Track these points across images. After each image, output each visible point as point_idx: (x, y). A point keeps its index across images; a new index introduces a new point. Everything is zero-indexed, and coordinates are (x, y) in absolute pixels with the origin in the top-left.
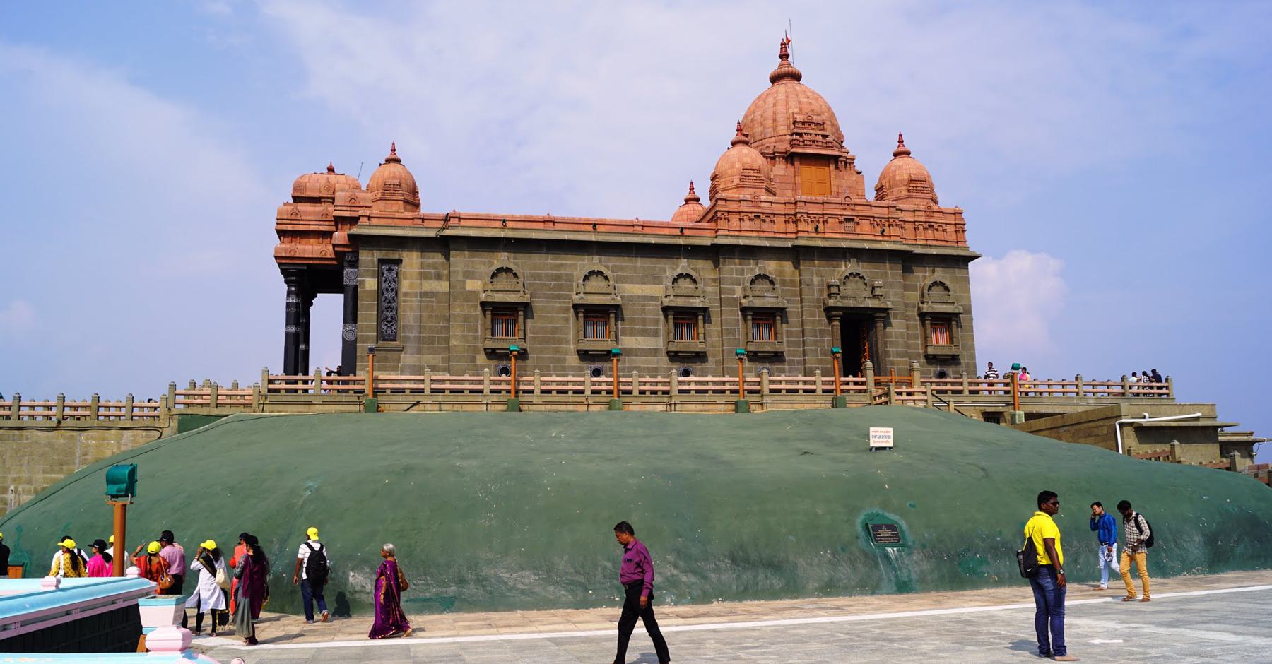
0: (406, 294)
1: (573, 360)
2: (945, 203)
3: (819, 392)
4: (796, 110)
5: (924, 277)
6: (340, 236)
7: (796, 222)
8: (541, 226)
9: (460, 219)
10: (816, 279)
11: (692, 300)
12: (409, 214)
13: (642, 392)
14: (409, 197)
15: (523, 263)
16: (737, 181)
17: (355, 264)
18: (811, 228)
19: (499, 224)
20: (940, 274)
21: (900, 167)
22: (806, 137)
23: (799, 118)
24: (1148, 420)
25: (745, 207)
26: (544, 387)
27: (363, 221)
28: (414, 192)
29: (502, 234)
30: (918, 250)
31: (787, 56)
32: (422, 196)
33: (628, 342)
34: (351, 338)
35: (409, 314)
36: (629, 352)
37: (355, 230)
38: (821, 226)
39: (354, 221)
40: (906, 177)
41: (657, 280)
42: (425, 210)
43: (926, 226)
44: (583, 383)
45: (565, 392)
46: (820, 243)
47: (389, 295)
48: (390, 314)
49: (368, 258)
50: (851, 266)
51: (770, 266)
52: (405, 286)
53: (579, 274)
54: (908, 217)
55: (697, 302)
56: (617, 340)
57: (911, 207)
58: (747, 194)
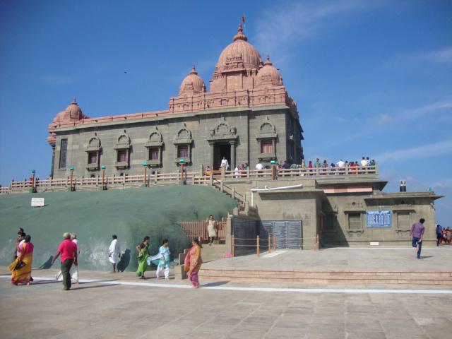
1: (115, 170)
5: (260, 120)
10: (206, 128)
13: (115, 183)
15: (102, 135)
23: (230, 57)
24: (265, 190)
25: (180, 101)
30: (253, 110)
36: (135, 166)
38: (211, 105)
50: (221, 120)
51: (189, 124)
52: (68, 148)
54: (255, 94)
56: (129, 162)
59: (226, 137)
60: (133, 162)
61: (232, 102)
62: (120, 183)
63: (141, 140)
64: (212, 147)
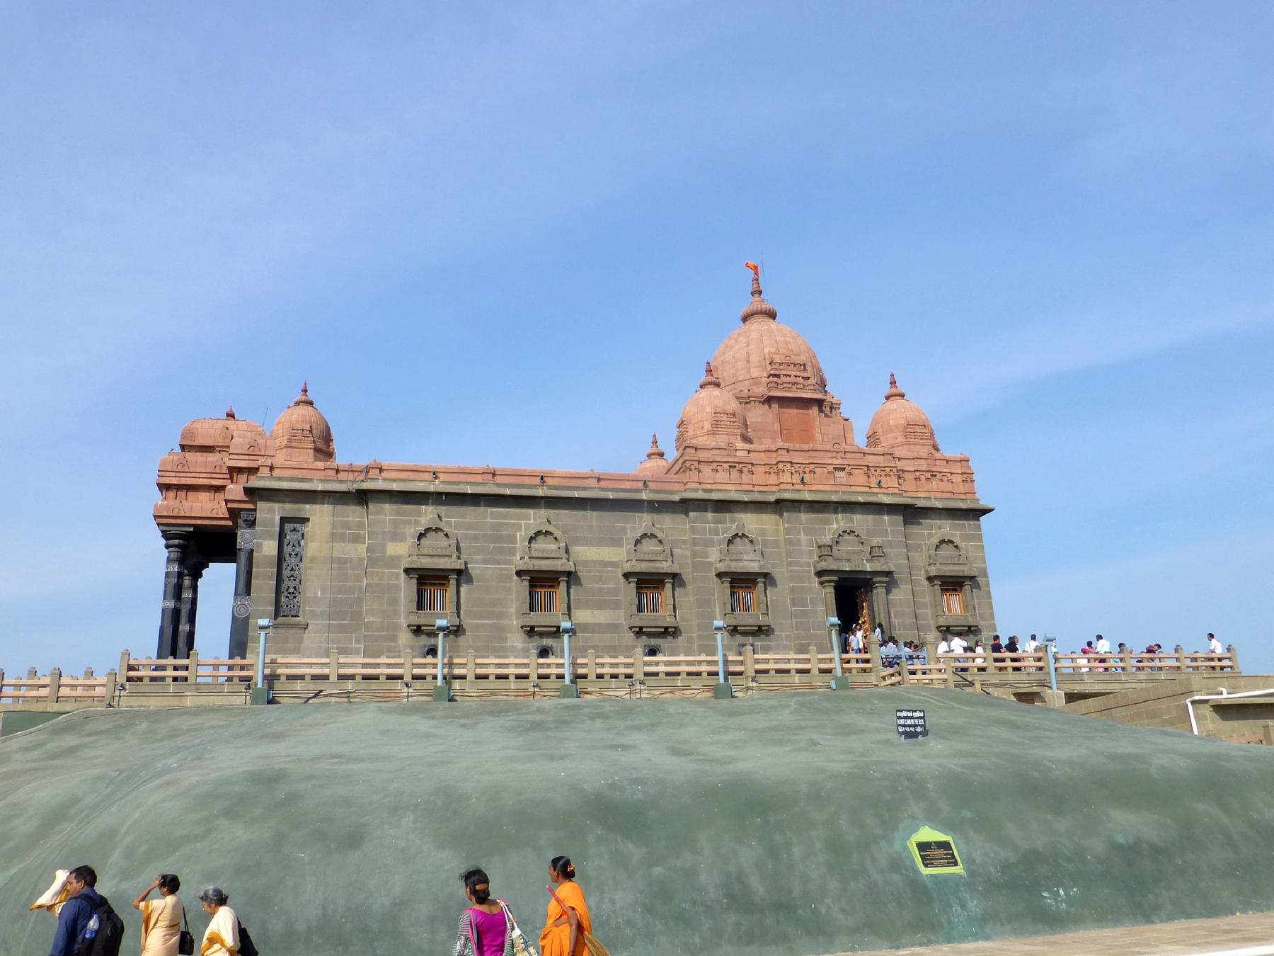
0: (313, 560)
1: (517, 640)
2: (948, 451)
3: (815, 672)
4: (773, 350)
6: (235, 490)
7: (777, 473)
8: (479, 478)
9: (381, 470)
11: (658, 565)
12: (320, 464)
13: (600, 677)
14: (320, 445)
15: (457, 519)
16: (708, 426)
17: (252, 524)
18: (797, 479)
19: (430, 476)
20: (946, 528)
21: (894, 410)
22: (783, 379)
23: (778, 359)
24: (1225, 696)
26: (479, 671)
27: (264, 472)
28: (327, 437)
29: (432, 488)
31: (760, 292)
32: (336, 446)
33: (583, 616)
34: (243, 613)
35: (315, 585)
36: (586, 627)
37: (254, 482)
38: (807, 478)
39: (253, 471)
40: (902, 421)
41: (617, 542)
42: (341, 459)
43: (928, 475)
44: (527, 665)
45: (506, 677)
46: (808, 497)
47: (293, 560)
48: (291, 584)
49: (269, 513)
51: (750, 522)
53: (521, 535)
54: (908, 466)
55: (665, 567)
57: (912, 455)
58: (721, 440)
59: (869, 567)
60: (583, 616)
61: (859, 476)
62: (614, 676)
63: (603, 552)
64: (830, 590)
